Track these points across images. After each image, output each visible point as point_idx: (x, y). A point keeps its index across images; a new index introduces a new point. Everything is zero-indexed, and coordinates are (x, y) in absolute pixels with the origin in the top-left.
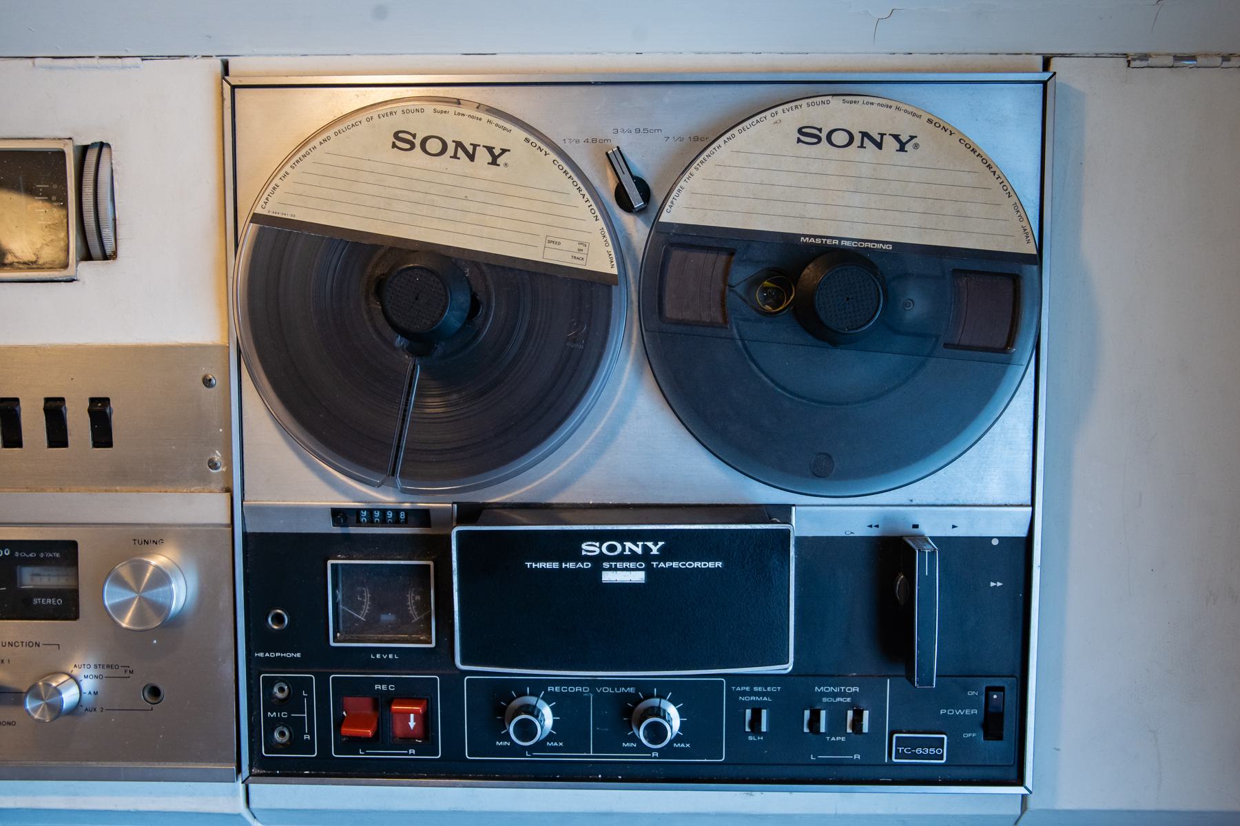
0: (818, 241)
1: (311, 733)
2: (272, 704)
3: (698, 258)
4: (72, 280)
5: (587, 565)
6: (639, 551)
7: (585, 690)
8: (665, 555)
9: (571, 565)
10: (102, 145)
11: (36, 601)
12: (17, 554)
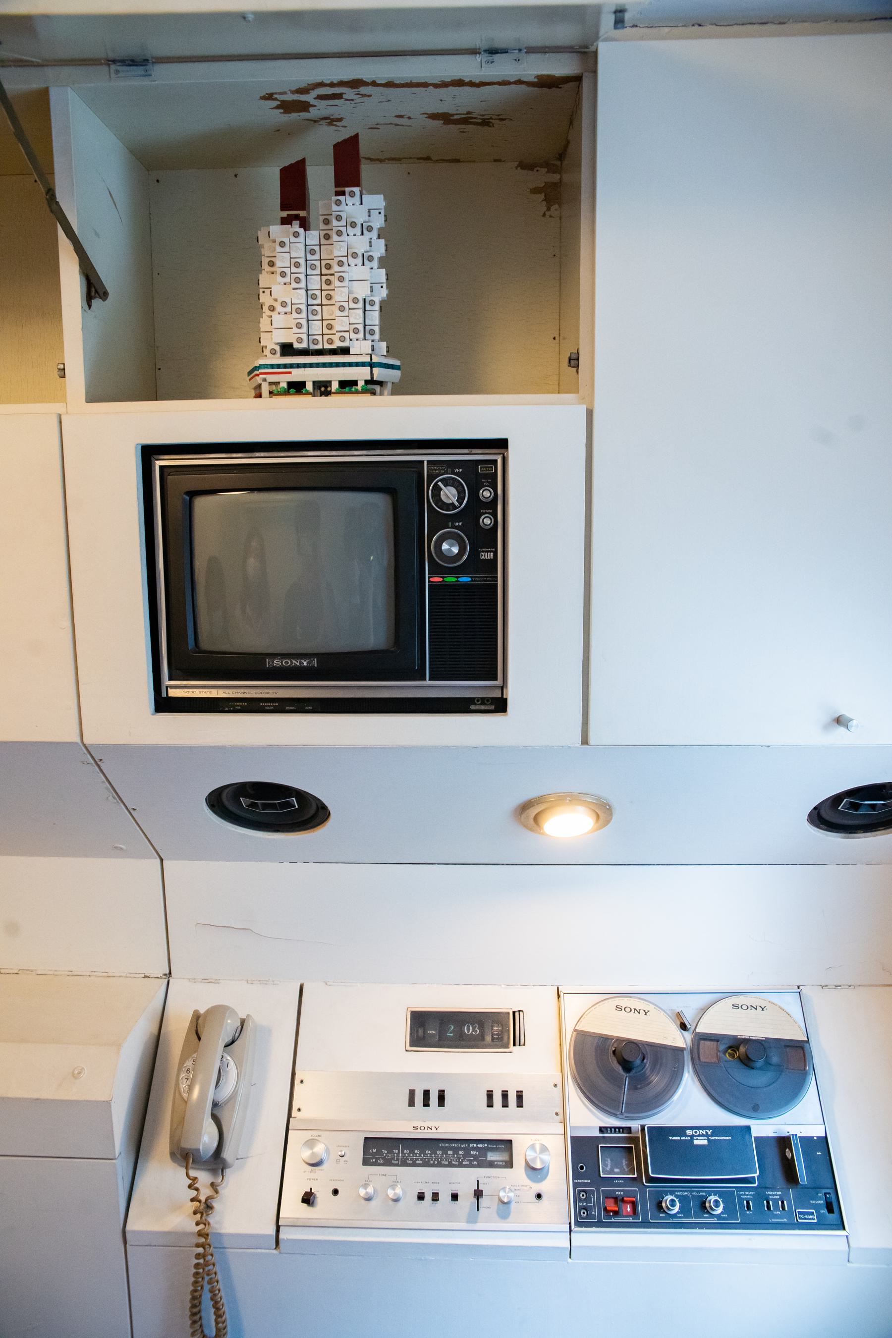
0: (743, 1037)
1: (595, 1211)
2: (581, 1200)
3: (708, 1043)
4: (511, 1052)
5: (689, 1138)
6: (704, 1133)
7: (689, 1194)
8: (712, 1135)
9: (684, 1138)
10: (519, 1011)
11: (495, 1163)
12: (489, 1146)
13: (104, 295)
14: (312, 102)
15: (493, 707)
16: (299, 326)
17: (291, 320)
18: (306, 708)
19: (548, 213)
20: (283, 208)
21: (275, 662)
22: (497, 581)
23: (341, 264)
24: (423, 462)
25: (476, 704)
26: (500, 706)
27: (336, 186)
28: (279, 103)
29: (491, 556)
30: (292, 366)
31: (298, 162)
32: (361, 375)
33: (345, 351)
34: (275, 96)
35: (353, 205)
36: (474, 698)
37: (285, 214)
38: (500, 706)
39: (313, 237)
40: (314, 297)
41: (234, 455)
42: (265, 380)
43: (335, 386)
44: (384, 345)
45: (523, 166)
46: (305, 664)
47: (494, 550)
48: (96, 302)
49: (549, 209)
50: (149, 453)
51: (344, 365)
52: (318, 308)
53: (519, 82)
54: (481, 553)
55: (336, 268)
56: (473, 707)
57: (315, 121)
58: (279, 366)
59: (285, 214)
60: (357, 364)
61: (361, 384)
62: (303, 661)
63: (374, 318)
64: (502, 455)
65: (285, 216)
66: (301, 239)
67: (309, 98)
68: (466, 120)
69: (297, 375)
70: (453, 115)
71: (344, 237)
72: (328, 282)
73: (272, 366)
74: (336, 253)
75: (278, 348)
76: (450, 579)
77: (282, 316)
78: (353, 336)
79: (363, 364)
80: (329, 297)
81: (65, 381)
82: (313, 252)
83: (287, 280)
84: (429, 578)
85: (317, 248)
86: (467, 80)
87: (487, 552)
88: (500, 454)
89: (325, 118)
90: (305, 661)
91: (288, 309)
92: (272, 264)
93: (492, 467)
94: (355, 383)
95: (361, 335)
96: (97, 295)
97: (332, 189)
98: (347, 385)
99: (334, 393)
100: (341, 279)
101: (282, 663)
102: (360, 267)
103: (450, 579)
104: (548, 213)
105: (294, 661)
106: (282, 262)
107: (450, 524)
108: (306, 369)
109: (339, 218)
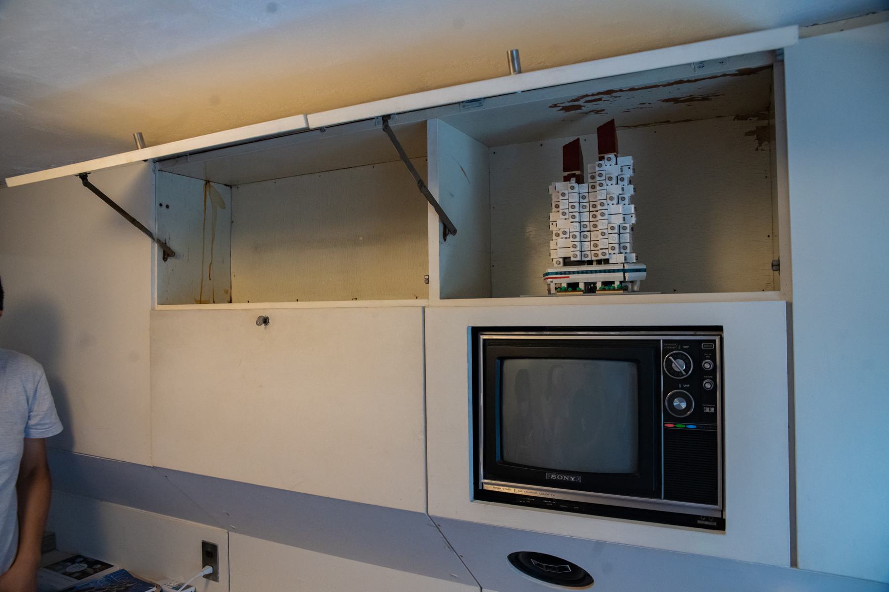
13: (454, 232)
14: (582, 104)
15: (715, 524)
16: (575, 246)
17: (569, 242)
18: (575, 508)
19: (760, 148)
20: (565, 170)
21: (552, 476)
22: (717, 429)
23: (602, 204)
24: (660, 340)
25: (702, 520)
26: (719, 525)
27: (599, 154)
28: (561, 108)
29: (712, 410)
30: (570, 273)
31: (574, 141)
32: (617, 277)
33: (607, 261)
34: (558, 105)
35: (610, 165)
36: (700, 516)
37: (566, 174)
38: (719, 525)
39: (584, 188)
40: (585, 226)
41: (530, 333)
42: (552, 282)
43: (599, 285)
44: (634, 255)
45: (738, 117)
46: (573, 479)
47: (714, 405)
48: (449, 237)
49: (760, 145)
50: (476, 332)
51: (605, 271)
52: (588, 234)
53: (725, 75)
54: (705, 408)
55: (599, 207)
56: (699, 522)
57: (586, 113)
58: (561, 273)
59: (566, 174)
60: (614, 271)
61: (617, 284)
62: (571, 477)
63: (627, 237)
64: (719, 336)
65: (567, 175)
66: (576, 190)
67: (581, 103)
68: (691, 99)
69: (573, 278)
70: (680, 98)
71: (605, 187)
72: (595, 216)
73: (557, 273)
74: (599, 197)
75: (561, 260)
76: (680, 426)
77: (564, 240)
78: (611, 251)
79: (618, 271)
80: (595, 226)
81: (428, 286)
82: (584, 197)
83: (567, 217)
84: (664, 424)
85: (586, 195)
86: (685, 80)
87: (709, 407)
88: (718, 335)
89: (593, 111)
90: (573, 477)
91: (567, 236)
92: (557, 206)
93: (712, 345)
94: (613, 283)
95: (617, 251)
96: (450, 233)
97: (597, 156)
99: (598, 290)
100: (603, 214)
101: (557, 477)
102: (616, 206)
103: (680, 426)
104: (760, 148)
105: (565, 477)
106: (564, 205)
107: (680, 386)
108: (579, 275)
109: (600, 175)
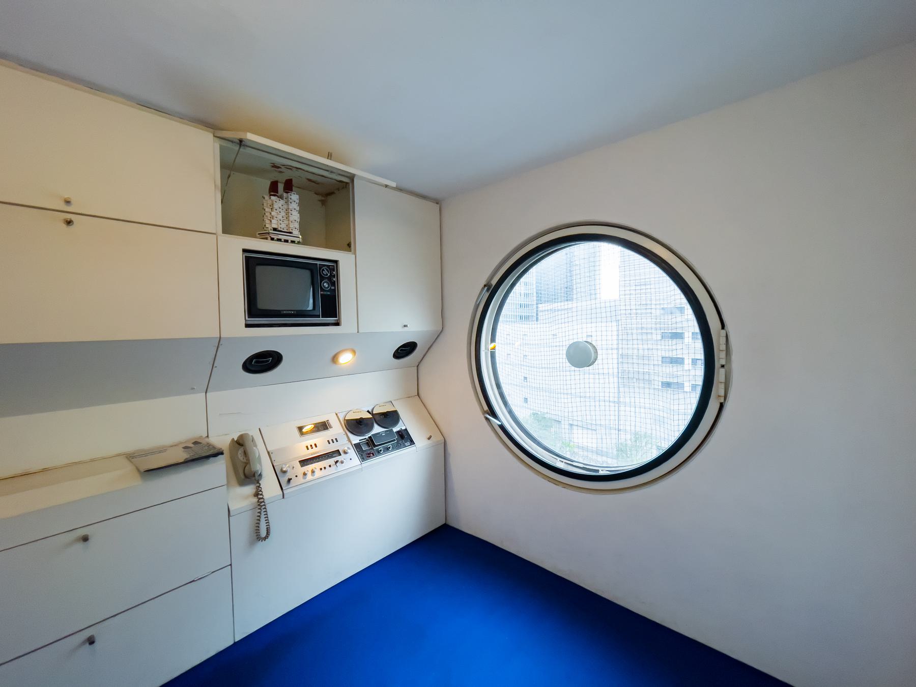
23: (291, 210)
38: (337, 324)
45: (316, 194)
98: (293, 242)
